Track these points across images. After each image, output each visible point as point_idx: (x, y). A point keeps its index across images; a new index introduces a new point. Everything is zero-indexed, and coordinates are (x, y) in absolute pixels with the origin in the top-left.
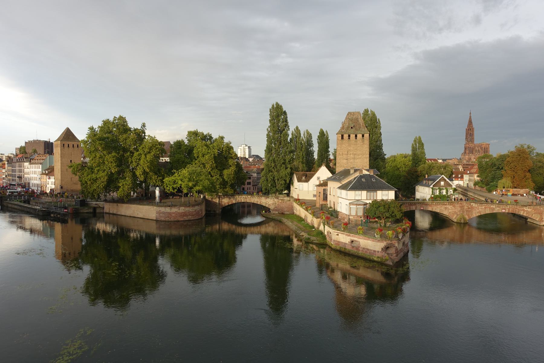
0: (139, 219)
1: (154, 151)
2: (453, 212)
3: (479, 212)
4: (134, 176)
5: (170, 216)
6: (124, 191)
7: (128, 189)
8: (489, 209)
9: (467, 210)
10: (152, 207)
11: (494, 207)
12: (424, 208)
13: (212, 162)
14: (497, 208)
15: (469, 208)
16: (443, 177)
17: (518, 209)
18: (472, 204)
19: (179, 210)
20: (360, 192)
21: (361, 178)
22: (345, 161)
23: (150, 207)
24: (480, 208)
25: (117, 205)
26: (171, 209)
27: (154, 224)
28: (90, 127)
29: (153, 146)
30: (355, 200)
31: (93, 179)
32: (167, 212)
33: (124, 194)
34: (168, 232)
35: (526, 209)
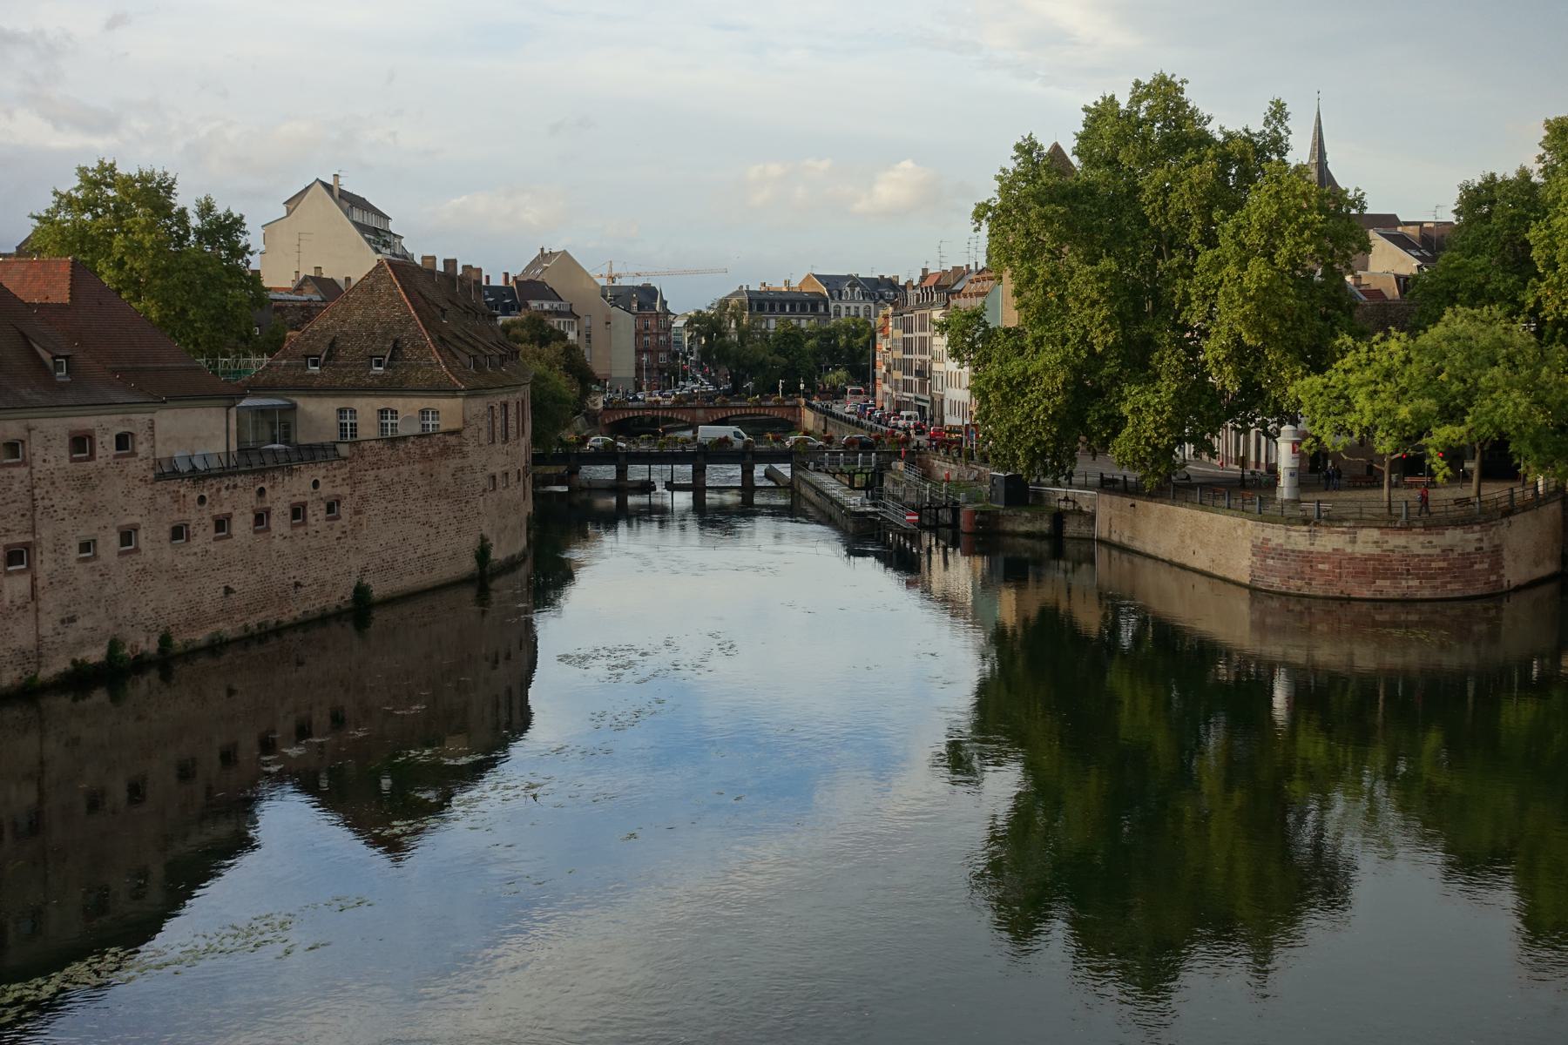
0: (1197, 576)
1: (1290, 242)
4: (1193, 368)
5: (1307, 570)
6: (1138, 443)
7: (1156, 429)
10: (1239, 520)
19: (1353, 541)
23: (1232, 520)
25: (1133, 505)
26: (1313, 535)
27: (1241, 605)
28: (1020, 140)
29: (1282, 212)
31: (1009, 381)
32: (1296, 548)
33: (1135, 452)
34: (1327, 654)
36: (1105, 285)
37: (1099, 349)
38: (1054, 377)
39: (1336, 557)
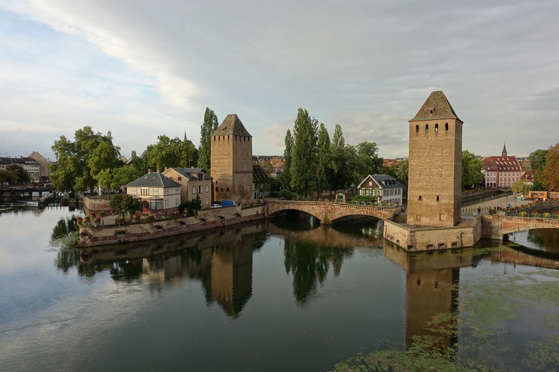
2: (319, 213)
3: (341, 214)
8: (349, 211)
9: (330, 210)
11: (354, 208)
12: (295, 207)
13: (159, 162)
14: (357, 210)
15: (332, 209)
16: (370, 177)
17: (376, 212)
18: (334, 205)
19: (101, 202)
22: (216, 161)
24: (341, 209)
31: (55, 176)
35: (383, 212)
36: (73, 160)
37: (72, 171)
38: (62, 176)
39: (99, 205)
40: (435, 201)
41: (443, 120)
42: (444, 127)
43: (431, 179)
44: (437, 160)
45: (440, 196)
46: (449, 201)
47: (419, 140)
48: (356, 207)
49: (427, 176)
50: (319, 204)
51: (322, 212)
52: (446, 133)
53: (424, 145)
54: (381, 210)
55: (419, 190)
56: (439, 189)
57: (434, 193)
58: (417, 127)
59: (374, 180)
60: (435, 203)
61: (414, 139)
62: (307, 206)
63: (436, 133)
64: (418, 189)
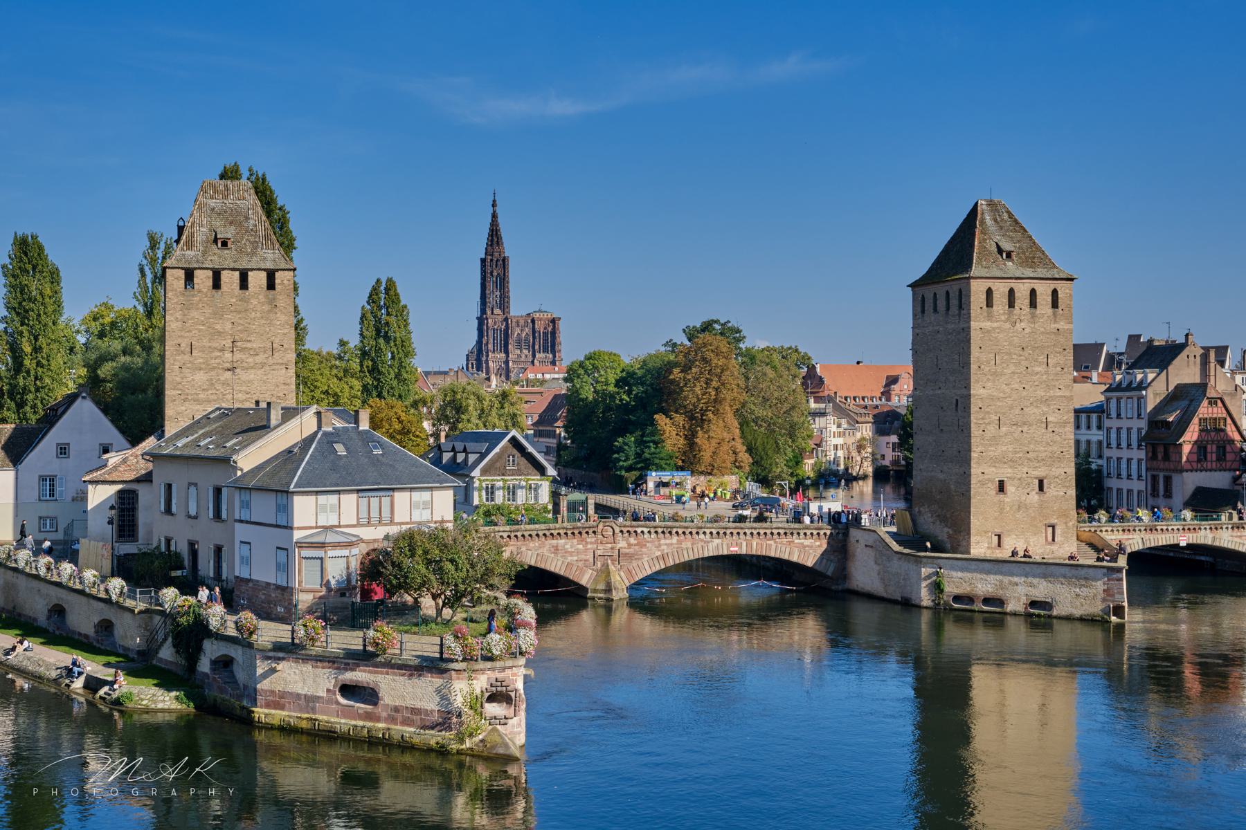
2: (580, 564)
9: (627, 551)
15: (630, 545)
18: (639, 530)
20: (333, 499)
21: (331, 443)
30: (317, 527)
40: (1034, 493)
41: (1051, 282)
42: (1049, 299)
43: (1025, 435)
44: (1036, 383)
45: (1045, 478)
46: (1064, 490)
47: (994, 329)
48: (714, 532)
49: (1014, 427)
50: (584, 532)
51: (591, 560)
52: (1054, 314)
53: (1005, 344)
54: (795, 536)
55: (997, 465)
56: (1043, 460)
57: (1034, 473)
58: (989, 292)
59: (530, 449)
60: (1035, 497)
61: (983, 325)
62: (534, 544)
63: (1033, 316)
64: (995, 461)
